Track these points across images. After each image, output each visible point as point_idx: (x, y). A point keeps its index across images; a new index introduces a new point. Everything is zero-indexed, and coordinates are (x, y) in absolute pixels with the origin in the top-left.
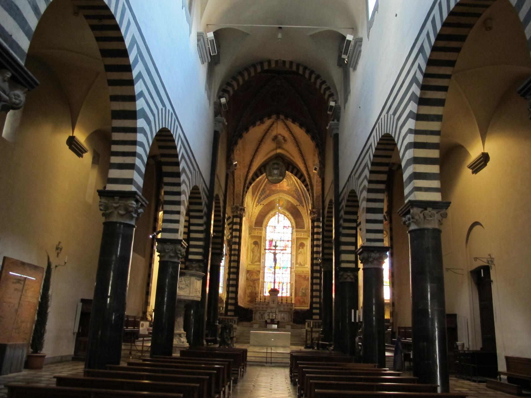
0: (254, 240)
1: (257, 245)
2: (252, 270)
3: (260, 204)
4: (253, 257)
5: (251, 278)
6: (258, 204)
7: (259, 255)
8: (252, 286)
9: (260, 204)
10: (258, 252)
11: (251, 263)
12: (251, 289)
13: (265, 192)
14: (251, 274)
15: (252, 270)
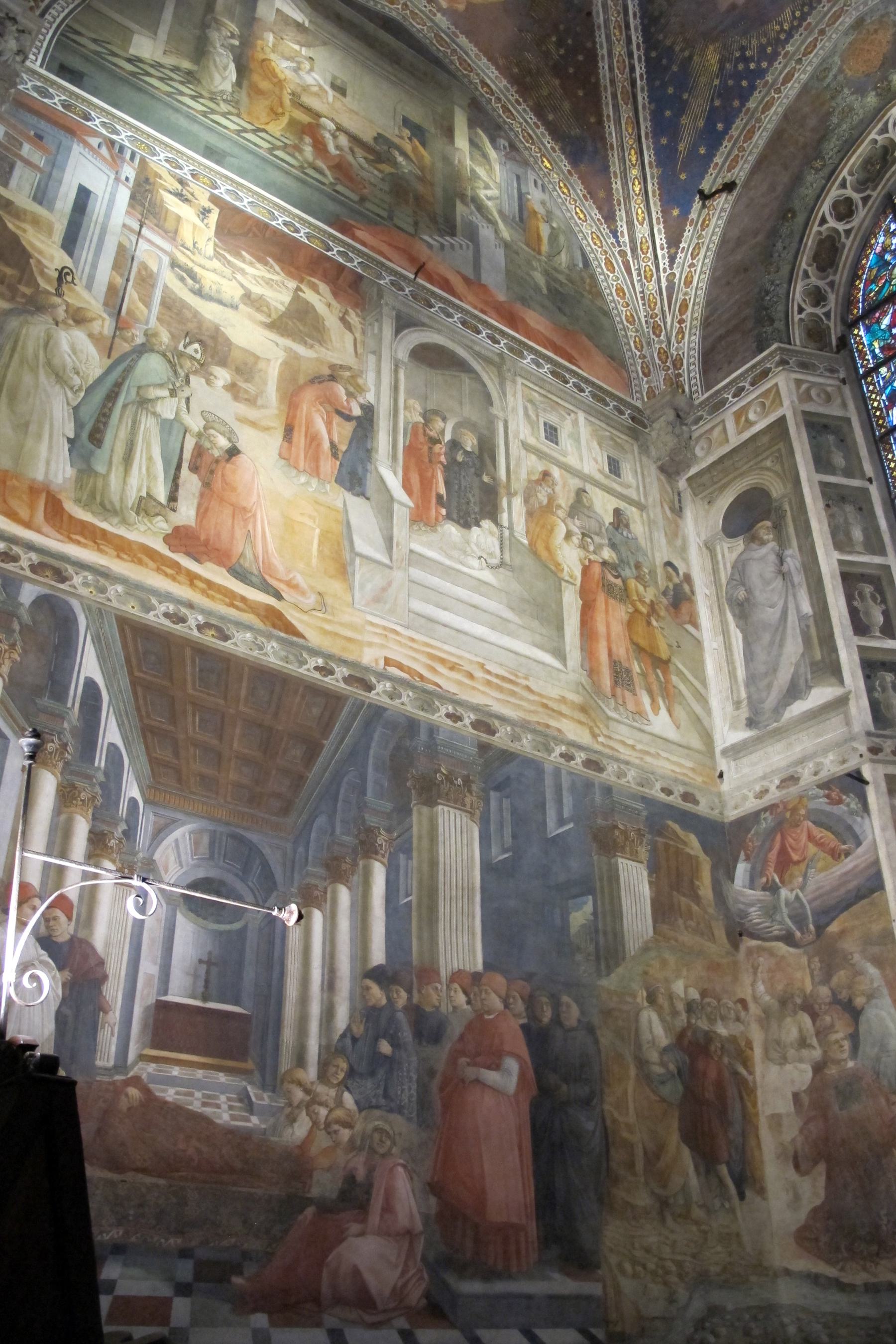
0: (725, 501)
1: (764, 529)
2: (774, 795)
3: (697, 204)
4: (749, 656)
5: (784, 893)
6: (686, 212)
7: (807, 608)
8: (810, 1008)
9: (697, 204)
10: (784, 575)
11: (751, 723)
12: (803, 1043)
13: (684, 81)
14: (773, 856)
15: (771, 808)
